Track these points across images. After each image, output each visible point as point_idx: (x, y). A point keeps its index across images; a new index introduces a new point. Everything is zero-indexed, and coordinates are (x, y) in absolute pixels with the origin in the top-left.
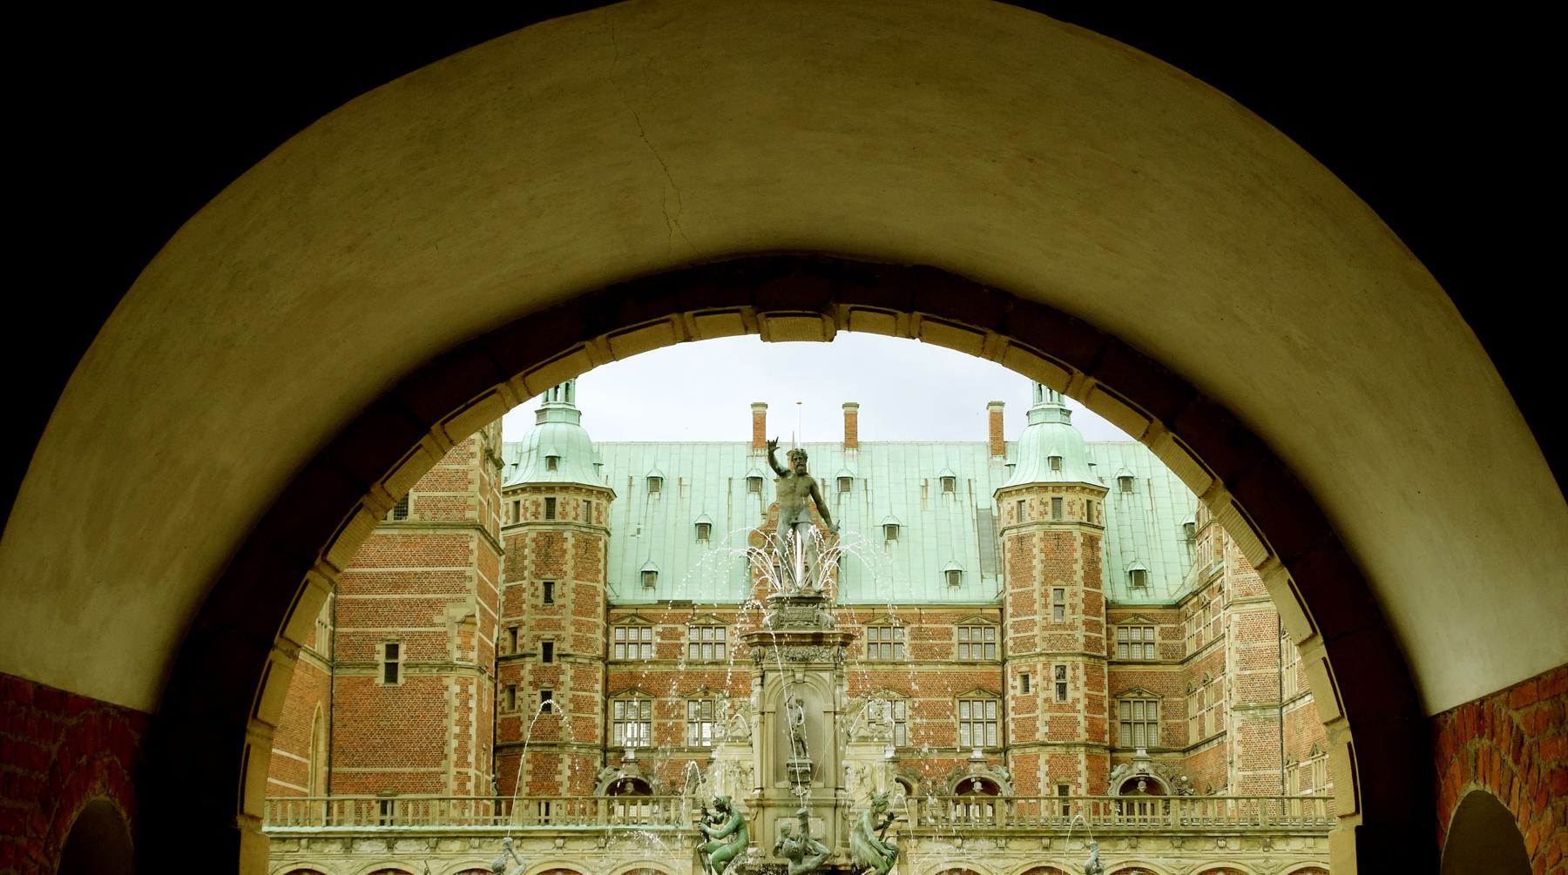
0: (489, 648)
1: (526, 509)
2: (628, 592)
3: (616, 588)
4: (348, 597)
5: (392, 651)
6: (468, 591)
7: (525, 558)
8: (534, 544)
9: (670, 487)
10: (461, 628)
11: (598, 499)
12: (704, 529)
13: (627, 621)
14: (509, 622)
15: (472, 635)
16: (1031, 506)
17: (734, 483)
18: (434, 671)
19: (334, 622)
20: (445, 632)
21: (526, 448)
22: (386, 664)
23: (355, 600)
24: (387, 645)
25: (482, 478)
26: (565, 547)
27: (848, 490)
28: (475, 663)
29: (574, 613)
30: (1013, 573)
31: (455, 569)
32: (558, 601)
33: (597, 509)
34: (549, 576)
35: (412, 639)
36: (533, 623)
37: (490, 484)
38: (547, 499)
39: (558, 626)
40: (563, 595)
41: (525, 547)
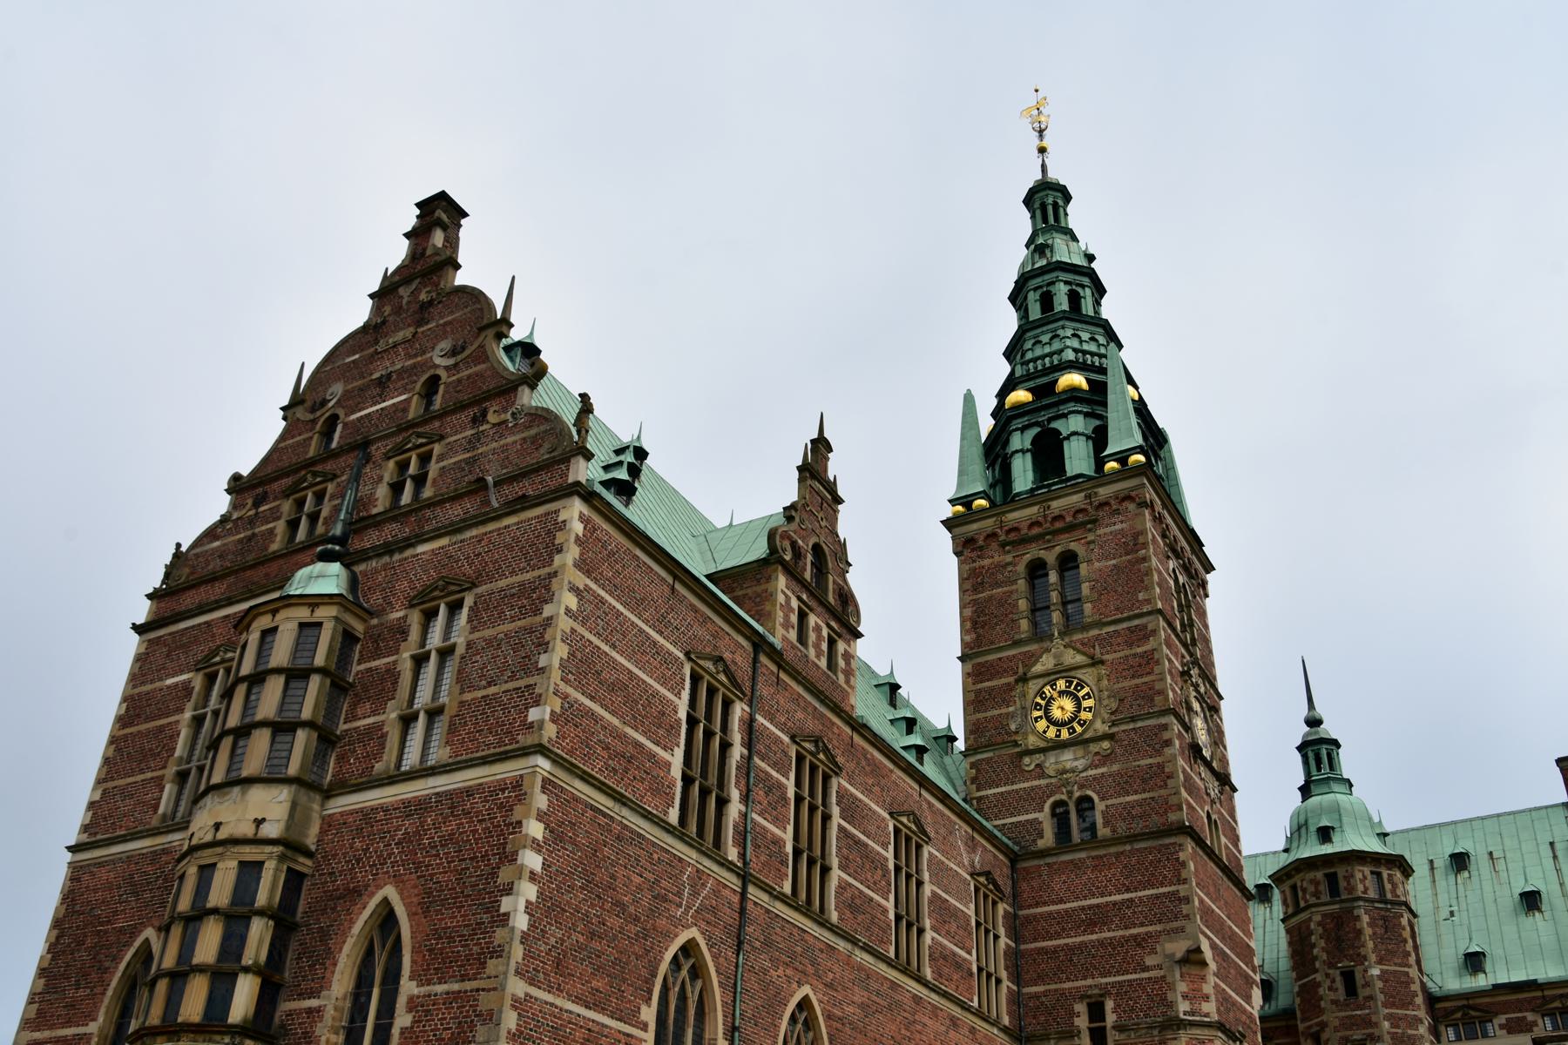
0: (1250, 1016)
1: (1304, 890)
2: (1453, 982)
3: (1437, 979)
4: (1033, 946)
5: (1096, 1012)
6: (1187, 917)
7: (1314, 946)
8: (1320, 930)
9: (1480, 863)
10: (1184, 970)
11: (1390, 869)
12: (1531, 901)
13: (1459, 1015)
14: (1310, 1027)
15: (1203, 978)
17: (1558, 846)
18: (1156, 1032)
19: (1016, 977)
20: (1164, 977)
21: (1296, 827)
22: (1090, 1029)
23: (1043, 948)
24: (1089, 1005)
25: (1187, 778)
26: (1358, 927)
28: (1215, 1017)
29: (1385, 1005)
31: (1162, 890)
32: (1363, 993)
34: (1346, 963)
35: (1121, 991)
36: (1337, 1023)
37: (1208, 794)
38: (1326, 875)
39: (1368, 1022)
40: (1367, 985)
41: (1311, 933)
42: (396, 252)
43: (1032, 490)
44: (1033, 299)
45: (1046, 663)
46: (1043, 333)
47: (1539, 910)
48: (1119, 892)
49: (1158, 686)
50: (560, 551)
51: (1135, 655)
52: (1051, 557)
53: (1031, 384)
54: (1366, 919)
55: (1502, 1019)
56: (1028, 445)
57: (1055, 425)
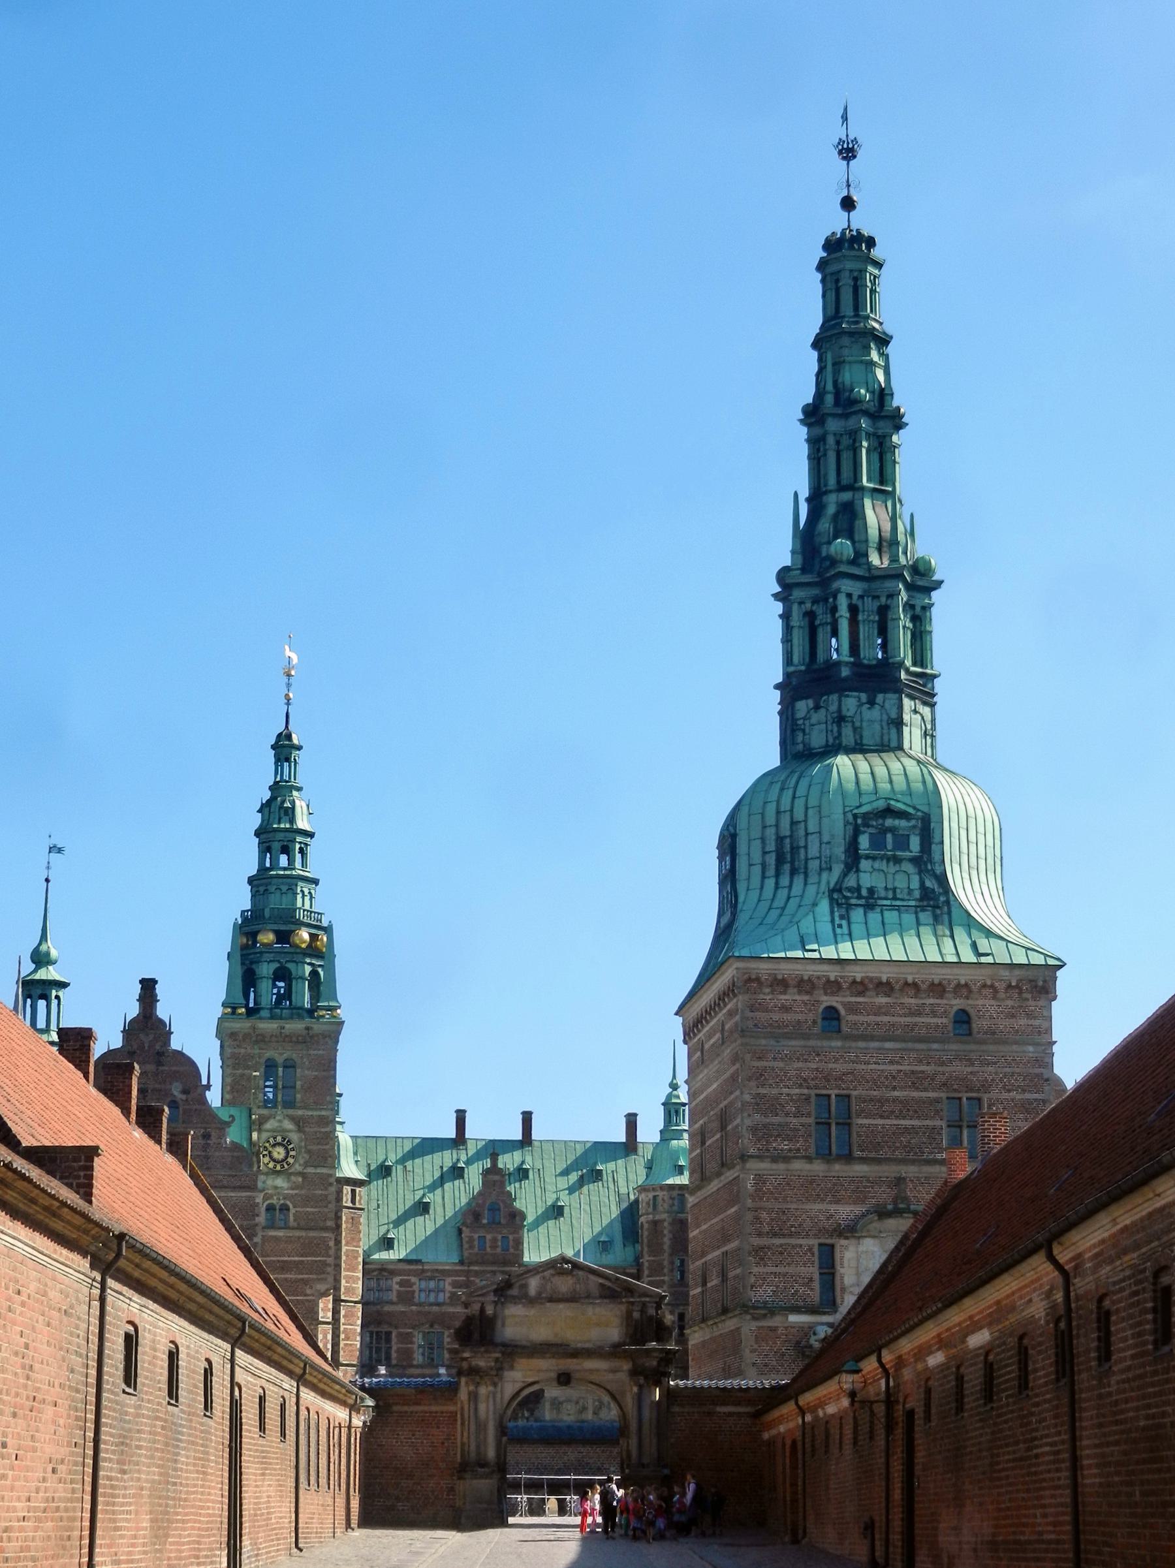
13: (375, 1273)
16: (663, 1200)
27: (527, 1177)
30: (649, 1246)
33: (360, 1195)
42: (134, 1010)
43: (271, 1009)
44: (276, 846)
45: (270, 1125)
46: (283, 884)
47: (428, 1212)
48: (297, 1256)
49: (331, 1153)
50: (258, 1215)
51: (320, 1132)
52: (280, 1060)
53: (276, 927)
54: (344, 1218)
55: (397, 1279)
56: (271, 972)
57: (289, 965)
